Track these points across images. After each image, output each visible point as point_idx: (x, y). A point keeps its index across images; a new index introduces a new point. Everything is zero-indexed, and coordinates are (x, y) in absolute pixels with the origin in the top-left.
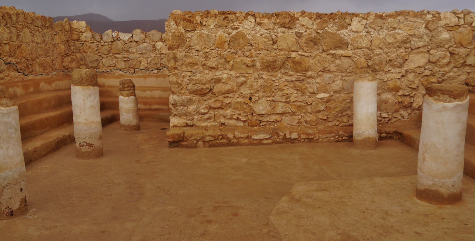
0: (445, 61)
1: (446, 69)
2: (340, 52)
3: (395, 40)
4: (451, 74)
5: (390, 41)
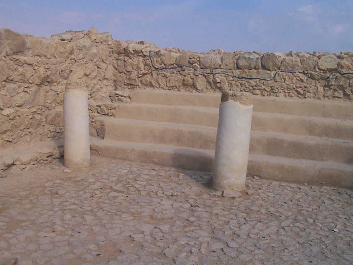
0: (94, 74)
1: (95, 81)
2: (23, 58)
3: (65, 50)
4: (98, 86)
5: (61, 51)
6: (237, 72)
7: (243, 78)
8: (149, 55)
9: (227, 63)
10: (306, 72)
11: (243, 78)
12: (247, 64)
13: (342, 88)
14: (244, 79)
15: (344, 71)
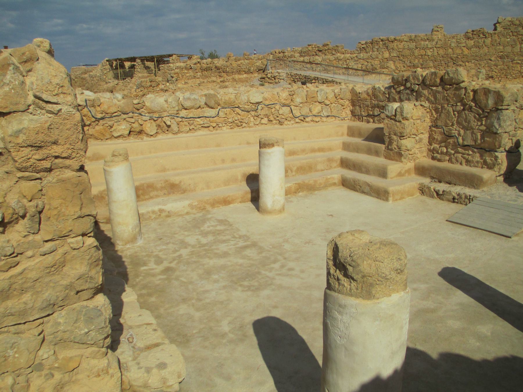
6: (183, 113)
7: (191, 118)
8: (85, 104)
9: (174, 106)
10: (240, 106)
11: (191, 118)
12: (192, 105)
13: (267, 116)
14: (192, 119)
15: (267, 103)
